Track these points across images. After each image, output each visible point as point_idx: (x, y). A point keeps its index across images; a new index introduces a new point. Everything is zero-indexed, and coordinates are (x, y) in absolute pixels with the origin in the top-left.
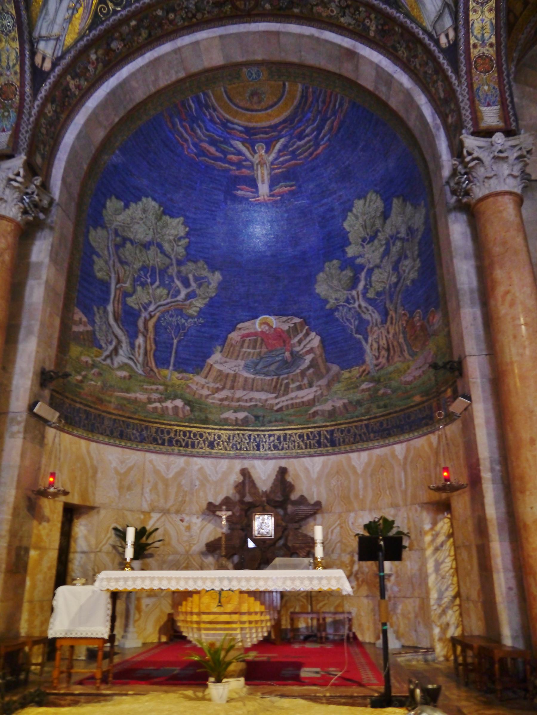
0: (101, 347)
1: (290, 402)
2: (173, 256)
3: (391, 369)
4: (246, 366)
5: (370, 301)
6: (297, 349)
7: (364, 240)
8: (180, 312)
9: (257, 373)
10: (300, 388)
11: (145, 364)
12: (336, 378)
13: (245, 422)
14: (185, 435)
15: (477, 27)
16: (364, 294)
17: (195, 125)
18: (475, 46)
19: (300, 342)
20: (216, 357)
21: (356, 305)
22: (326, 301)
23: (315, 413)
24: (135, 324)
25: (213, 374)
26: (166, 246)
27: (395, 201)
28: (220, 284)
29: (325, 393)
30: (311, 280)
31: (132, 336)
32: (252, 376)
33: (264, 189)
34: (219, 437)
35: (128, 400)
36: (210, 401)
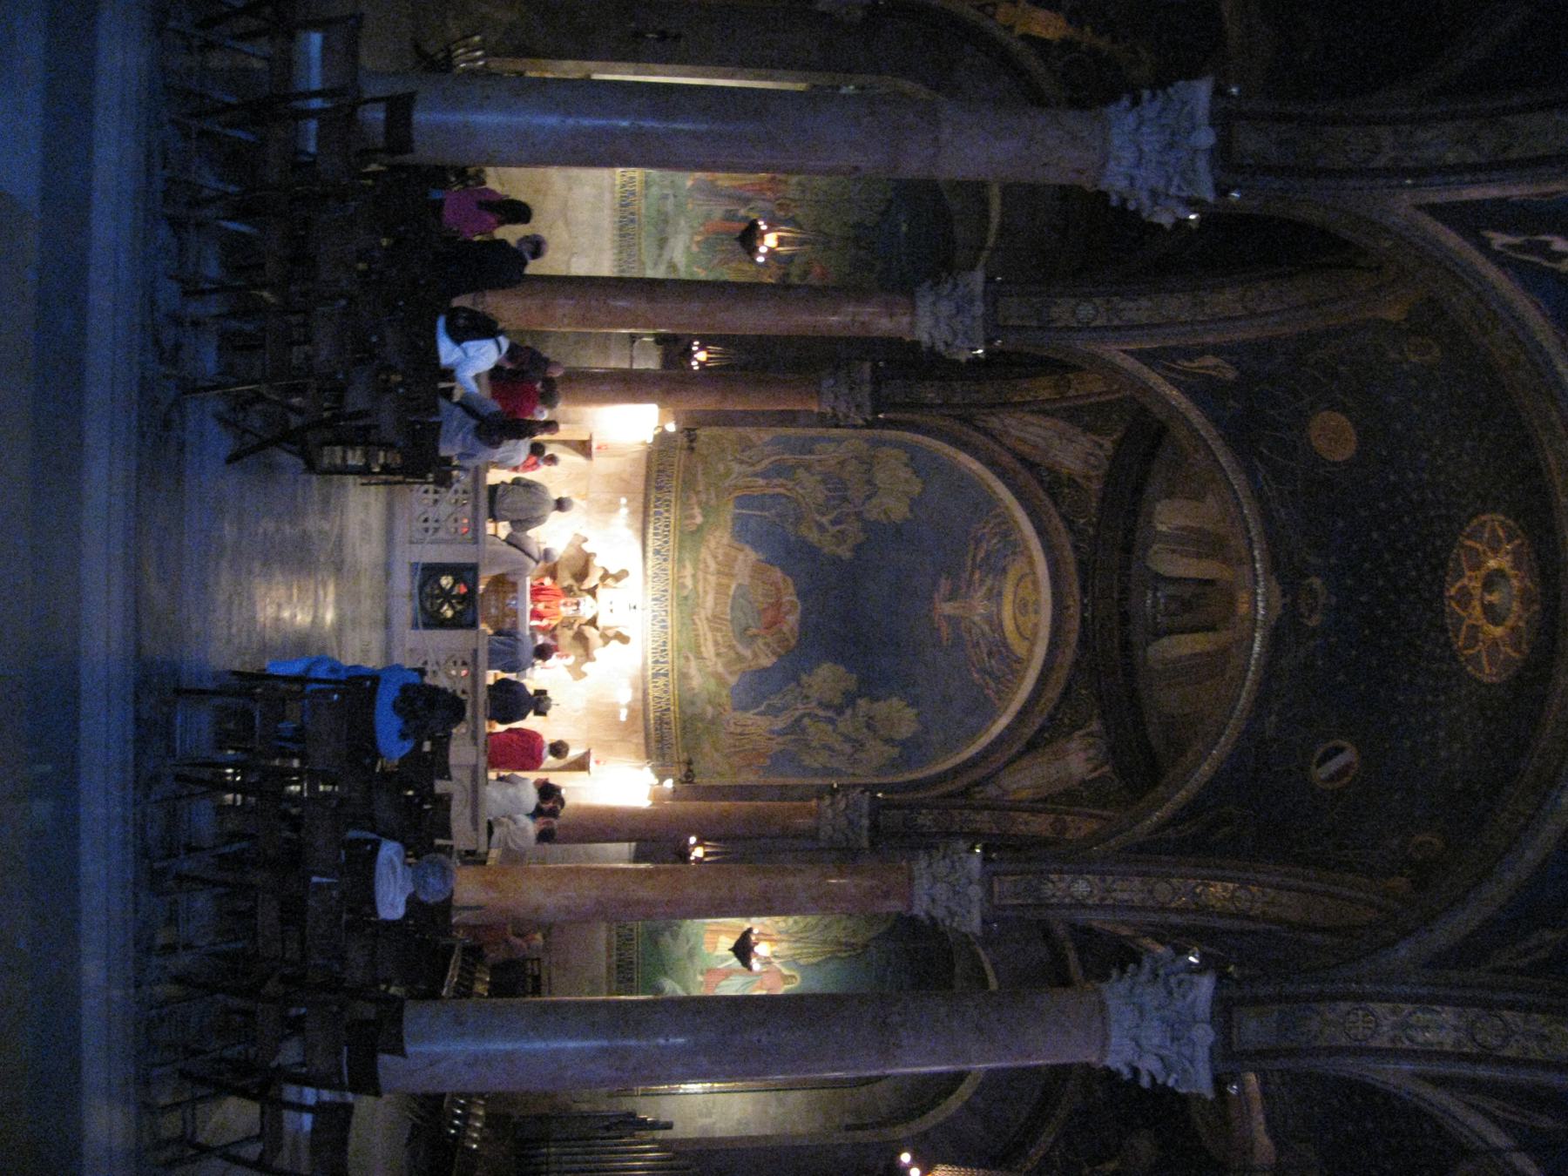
0: (743, 451)
1: (701, 632)
2: (867, 507)
3: (722, 736)
4: (740, 586)
5: (798, 720)
6: (760, 642)
7: (870, 718)
8: (799, 520)
9: (734, 598)
10: (716, 643)
11: (736, 488)
12: (720, 679)
13: (683, 586)
14: (667, 526)
15: (978, 818)
16: (809, 715)
17: (998, 538)
18: (961, 814)
19: (766, 644)
20: (753, 556)
21: (800, 706)
22: (810, 672)
23: (687, 658)
24: (779, 475)
25: (733, 552)
26: (874, 501)
27: (897, 750)
28: (839, 558)
29: (709, 670)
30: (838, 658)
31: (764, 475)
32: (731, 593)
33: (948, 608)
34: (665, 560)
35: (695, 476)
36: (703, 550)
